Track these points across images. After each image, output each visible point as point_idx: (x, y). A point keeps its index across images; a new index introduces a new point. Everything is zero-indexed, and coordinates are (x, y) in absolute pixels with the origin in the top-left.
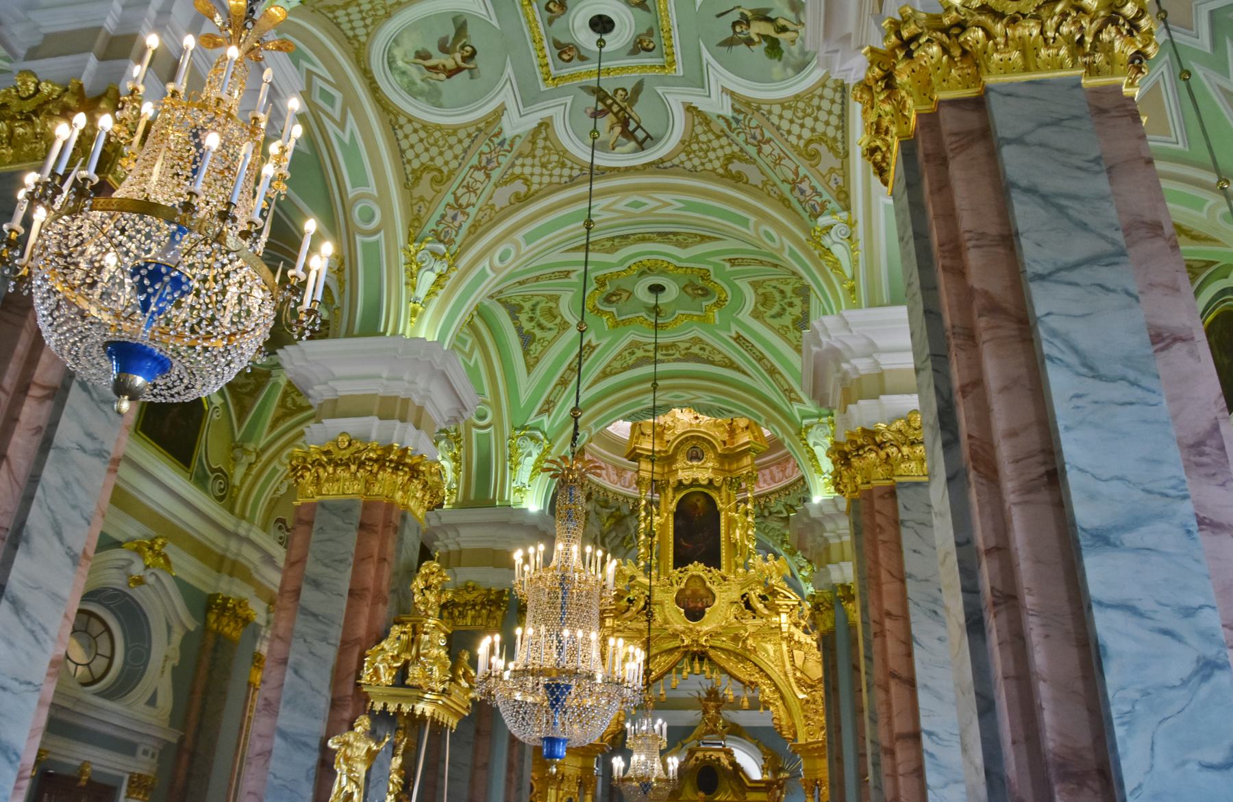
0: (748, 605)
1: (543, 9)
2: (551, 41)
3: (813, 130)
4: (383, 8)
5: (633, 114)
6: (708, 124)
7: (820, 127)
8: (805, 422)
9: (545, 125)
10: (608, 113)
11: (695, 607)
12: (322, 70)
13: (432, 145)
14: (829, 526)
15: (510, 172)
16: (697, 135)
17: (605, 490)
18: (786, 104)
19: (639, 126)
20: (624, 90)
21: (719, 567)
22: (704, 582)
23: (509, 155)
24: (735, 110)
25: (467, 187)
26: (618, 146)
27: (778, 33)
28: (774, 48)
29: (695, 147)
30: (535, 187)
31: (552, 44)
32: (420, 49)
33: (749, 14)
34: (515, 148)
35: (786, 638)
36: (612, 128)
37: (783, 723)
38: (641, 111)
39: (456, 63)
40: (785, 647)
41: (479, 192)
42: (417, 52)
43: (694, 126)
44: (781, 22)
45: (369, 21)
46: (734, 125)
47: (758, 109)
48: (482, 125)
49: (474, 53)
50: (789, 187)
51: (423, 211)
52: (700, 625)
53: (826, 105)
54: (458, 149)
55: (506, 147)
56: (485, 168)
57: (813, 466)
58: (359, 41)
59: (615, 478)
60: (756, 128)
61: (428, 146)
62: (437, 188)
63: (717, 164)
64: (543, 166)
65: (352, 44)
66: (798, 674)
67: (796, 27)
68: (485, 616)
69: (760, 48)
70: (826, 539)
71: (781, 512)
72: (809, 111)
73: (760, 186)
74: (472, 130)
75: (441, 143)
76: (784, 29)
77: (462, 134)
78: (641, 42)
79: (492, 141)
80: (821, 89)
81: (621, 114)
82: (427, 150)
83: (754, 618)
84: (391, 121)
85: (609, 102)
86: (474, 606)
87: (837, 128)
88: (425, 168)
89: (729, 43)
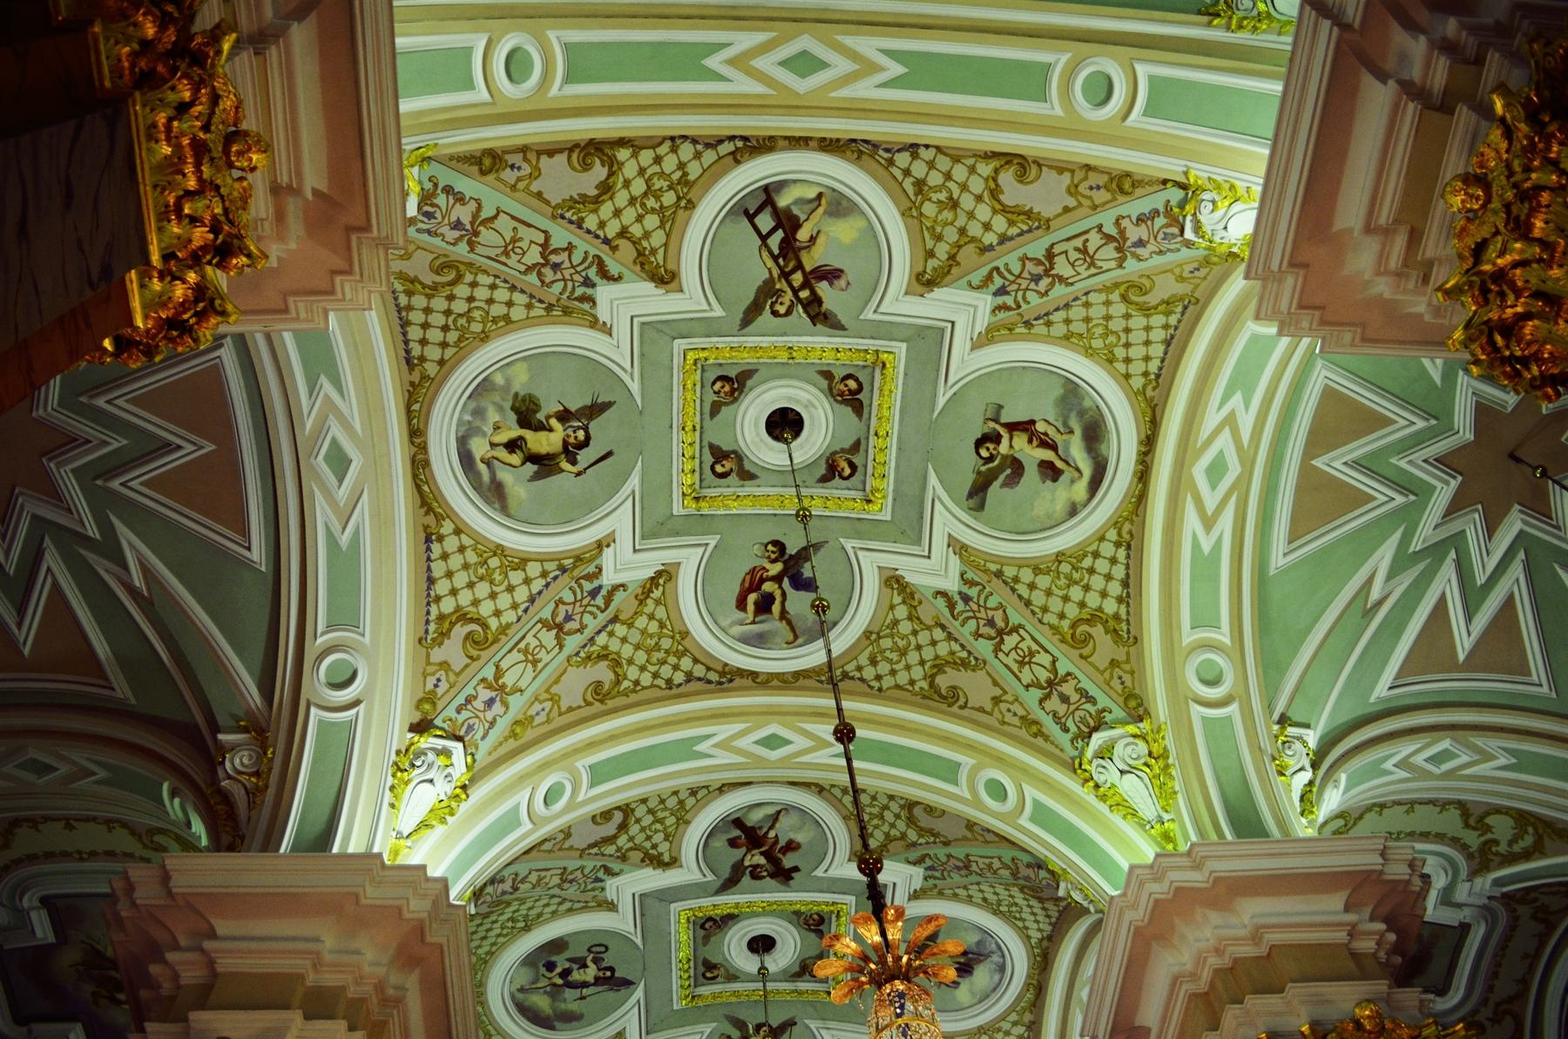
1: (860, 469)
2: (865, 415)
3: (451, 298)
4: (1058, 573)
5: (770, 263)
6: (640, 254)
7: (439, 303)
9: (925, 282)
10: (812, 272)
12: (1191, 522)
13: (1116, 333)
15: (1014, 231)
16: (662, 226)
18: (502, 323)
19: (764, 238)
20: (775, 313)
23: (1000, 263)
24: (591, 300)
25: (1092, 264)
26: (810, 201)
27: (521, 438)
28: (527, 414)
29: (669, 198)
30: (985, 169)
31: (866, 410)
32: (1049, 483)
33: (565, 465)
34: (984, 271)
36: (813, 239)
38: (757, 268)
39: (1011, 439)
41: (1078, 243)
42: (1055, 480)
43: (666, 245)
44: (515, 459)
45: (1088, 562)
46: (592, 273)
47: (549, 308)
48: (1021, 330)
49: (979, 443)
50: (485, 214)
51: (1188, 268)
53: (435, 335)
54: (1077, 312)
55: (998, 282)
56: (1047, 273)
58: (1119, 534)
60: (553, 282)
61: (1123, 336)
62: (1147, 283)
63: (630, 170)
64: (954, 204)
65: (1130, 533)
67: (495, 453)
69: (549, 407)
72: (462, 321)
73: (544, 158)
74: (1040, 328)
75: (1099, 330)
76: (513, 446)
77: (1059, 329)
78: (733, 391)
79: (1016, 301)
80: (446, 357)
81: (791, 265)
82: (1127, 330)
84: (1154, 389)
85: (804, 294)
87: (409, 308)
88: (1146, 310)
89: (596, 409)
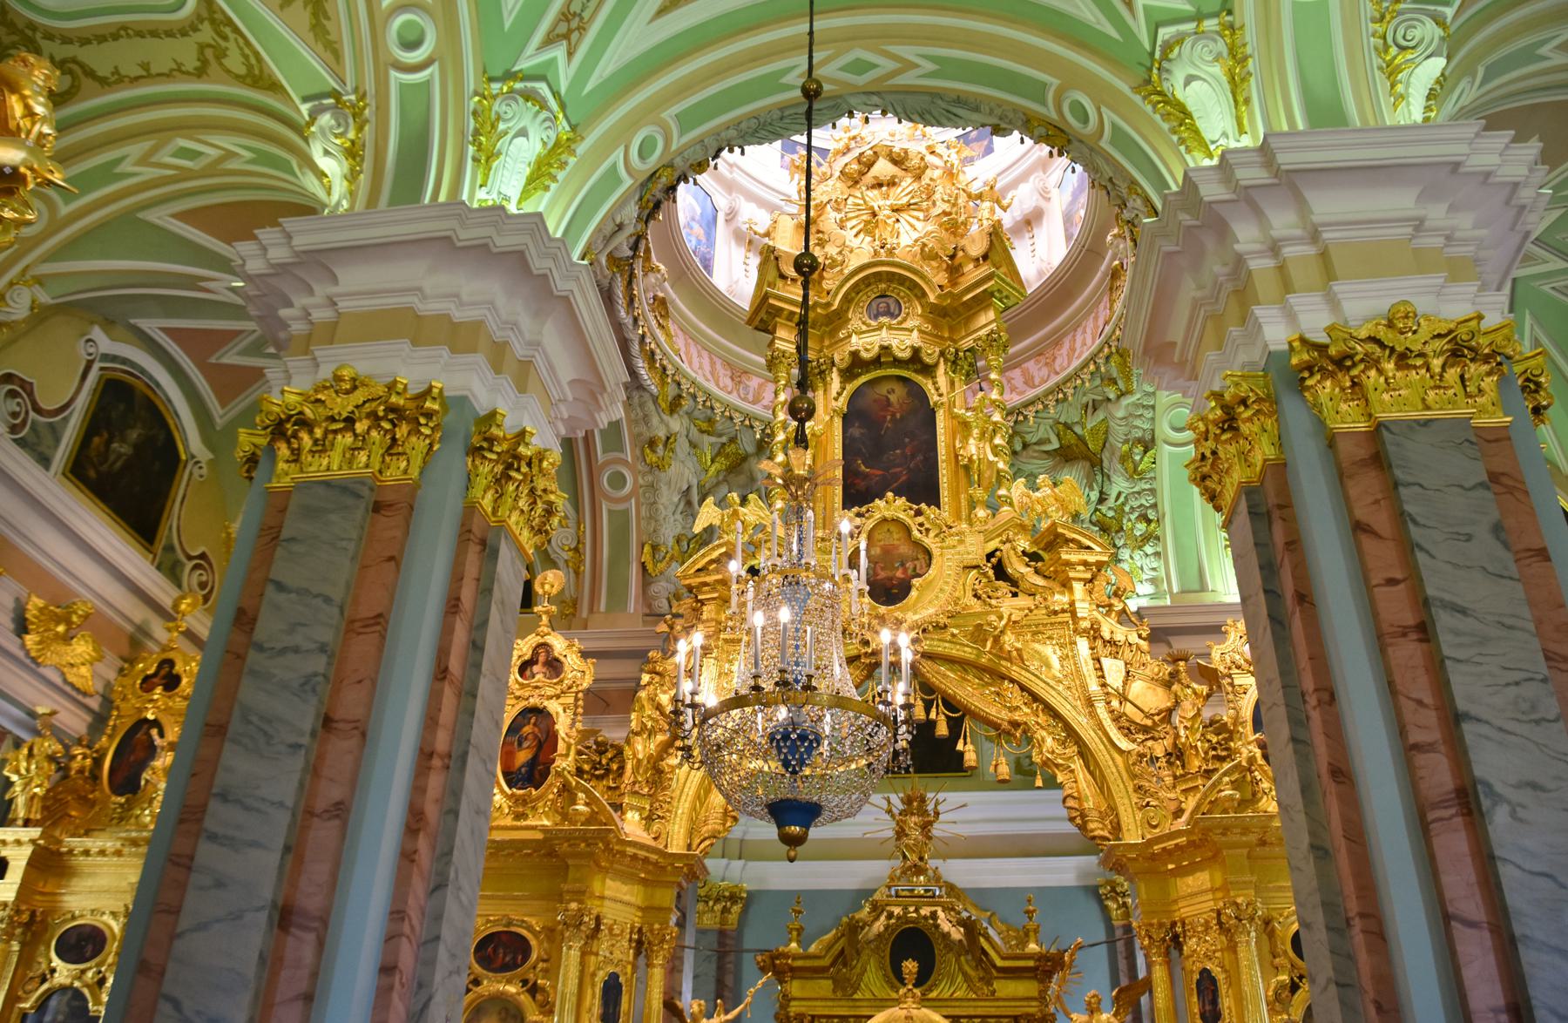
0: (1000, 572)
8: (1165, 33)
11: (891, 579)
14: (1246, 236)
17: (709, 396)
21: (934, 500)
22: (908, 530)
35: (1085, 631)
37: (1089, 804)
40: (1083, 645)
52: (904, 610)
57: (1182, 141)
59: (728, 382)
66: (1115, 703)
68: (378, 451)
70: (1240, 261)
71: (1048, 441)
83: (1015, 595)
86: (350, 421)
